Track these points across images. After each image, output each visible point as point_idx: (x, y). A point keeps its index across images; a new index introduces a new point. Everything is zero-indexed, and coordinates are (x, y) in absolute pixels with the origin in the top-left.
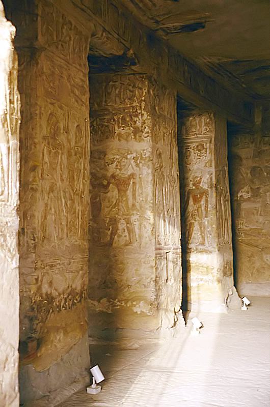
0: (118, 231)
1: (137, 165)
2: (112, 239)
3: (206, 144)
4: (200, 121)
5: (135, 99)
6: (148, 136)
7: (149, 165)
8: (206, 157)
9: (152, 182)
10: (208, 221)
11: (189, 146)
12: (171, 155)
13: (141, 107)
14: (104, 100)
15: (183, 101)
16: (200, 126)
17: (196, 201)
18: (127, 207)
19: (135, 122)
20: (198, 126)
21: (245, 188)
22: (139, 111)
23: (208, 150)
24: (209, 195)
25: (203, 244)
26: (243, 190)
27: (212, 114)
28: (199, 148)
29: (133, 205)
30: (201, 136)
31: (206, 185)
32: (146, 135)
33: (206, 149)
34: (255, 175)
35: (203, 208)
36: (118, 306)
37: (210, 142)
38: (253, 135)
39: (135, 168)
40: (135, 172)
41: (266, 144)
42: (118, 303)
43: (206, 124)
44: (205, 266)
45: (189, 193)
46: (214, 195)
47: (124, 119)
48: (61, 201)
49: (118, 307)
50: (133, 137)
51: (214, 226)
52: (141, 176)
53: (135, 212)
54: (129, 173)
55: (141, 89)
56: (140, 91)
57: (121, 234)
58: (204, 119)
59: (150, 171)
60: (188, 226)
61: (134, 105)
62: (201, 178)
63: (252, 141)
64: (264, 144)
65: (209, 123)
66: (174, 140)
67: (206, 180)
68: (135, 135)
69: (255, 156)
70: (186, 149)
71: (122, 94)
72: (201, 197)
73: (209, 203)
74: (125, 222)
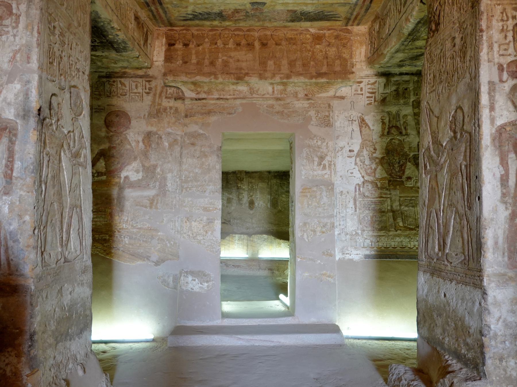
3: (18, 5)
8: (15, 36)
21: (133, 165)
24: (19, 136)
26: (130, 167)
31: (12, 111)
33: (18, 16)
34: (150, 146)
38: (149, 81)
41: (169, 98)
46: (33, 136)
63: (147, 91)
64: (166, 98)
67: (11, 97)
69: (150, 115)
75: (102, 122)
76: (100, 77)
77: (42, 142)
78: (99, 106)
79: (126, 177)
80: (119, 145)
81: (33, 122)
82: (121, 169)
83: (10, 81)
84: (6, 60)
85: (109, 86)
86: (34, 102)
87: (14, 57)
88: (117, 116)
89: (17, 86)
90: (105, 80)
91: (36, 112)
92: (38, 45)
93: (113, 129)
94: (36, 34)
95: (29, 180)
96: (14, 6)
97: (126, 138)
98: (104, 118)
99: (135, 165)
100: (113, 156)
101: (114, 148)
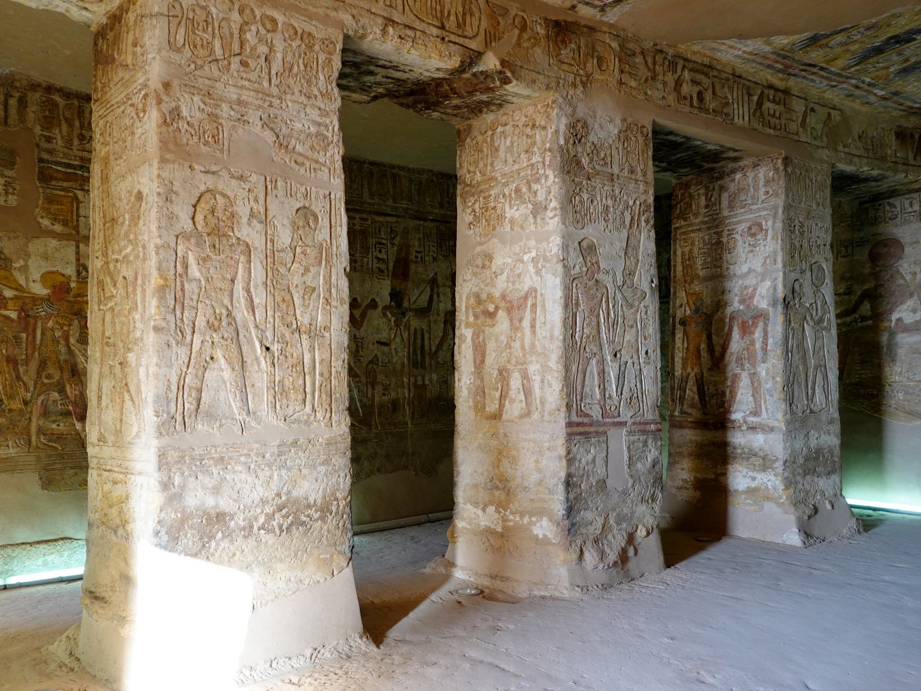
0: (510, 393)
1: (538, 272)
2: (501, 405)
3: (766, 222)
4: (756, 178)
5: (535, 149)
6: (555, 216)
7: (556, 270)
8: (765, 246)
9: (563, 301)
10: (768, 369)
11: (733, 230)
12: (629, 248)
13: (544, 163)
14: (489, 162)
15: (699, 143)
16: (756, 189)
17: (746, 330)
18: (523, 348)
19: (535, 193)
20: (752, 189)
22: (541, 172)
23: (770, 232)
25: (755, 413)
26: (904, 307)
27: (780, 161)
28: (753, 231)
29: (533, 346)
30: (756, 207)
32: (551, 214)
35: (758, 345)
36: (510, 521)
37: (775, 217)
39: (535, 278)
40: (535, 285)
42: (511, 517)
43: (767, 182)
44: (761, 453)
45: (732, 318)
46: (780, 319)
47: (518, 190)
48: (253, 345)
49: (512, 523)
50: (532, 221)
51: (778, 379)
52: (543, 292)
53: (534, 358)
54: (526, 288)
55: (544, 128)
56: (543, 133)
57: (513, 397)
58: (764, 172)
59: (558, 281)
60: (730, 380)
61: (534, 160)
62: (755, 289)
65: (773, 180)
66: (643, 219)
68: (535, 217)
70: (729, 235)
71: (515, 144)
72: (755, 324)
73: (769, 335)
74: (519, 377)
75: (866, 256)
76: (861, 203)
77: (787, 321)
78: (861, 238)
79: (899, 320)
80: (888, 280)
81: (780, 308)
82: (891, 311)
83: (763, 280)
84: (760, 265)
85: (873, 212)
86: (780, 294)
87: (765, 262)
88: (885, 246)
89: (768, 283)
90: (867, 205)
91: (782, 300)
92: (782, 249)
93: (880, 263)
94: (780, 241)
95: (779, 352)
96: (764, 223)
97: (898, 271)
98: (867, 251)
99: (910, 303)
100: (881, 296)
101: (882, 285)
